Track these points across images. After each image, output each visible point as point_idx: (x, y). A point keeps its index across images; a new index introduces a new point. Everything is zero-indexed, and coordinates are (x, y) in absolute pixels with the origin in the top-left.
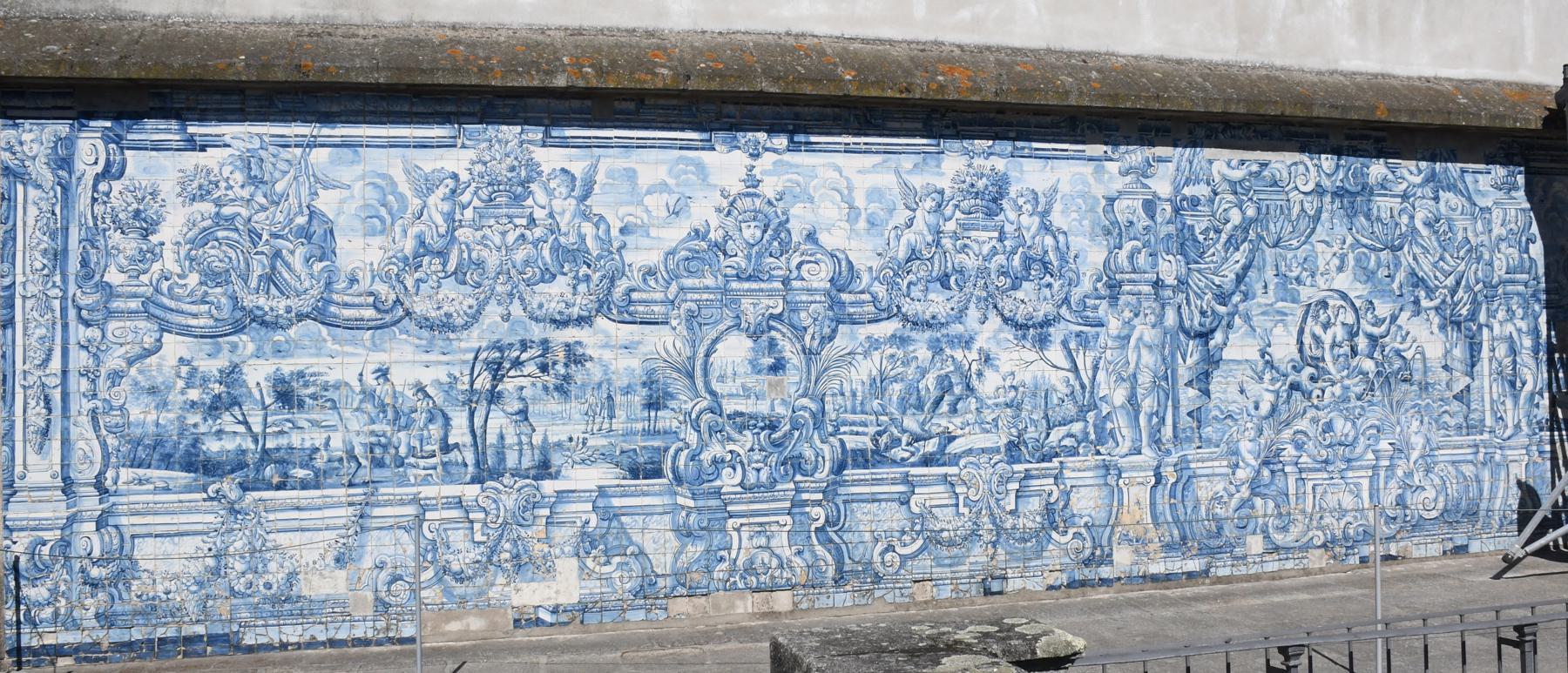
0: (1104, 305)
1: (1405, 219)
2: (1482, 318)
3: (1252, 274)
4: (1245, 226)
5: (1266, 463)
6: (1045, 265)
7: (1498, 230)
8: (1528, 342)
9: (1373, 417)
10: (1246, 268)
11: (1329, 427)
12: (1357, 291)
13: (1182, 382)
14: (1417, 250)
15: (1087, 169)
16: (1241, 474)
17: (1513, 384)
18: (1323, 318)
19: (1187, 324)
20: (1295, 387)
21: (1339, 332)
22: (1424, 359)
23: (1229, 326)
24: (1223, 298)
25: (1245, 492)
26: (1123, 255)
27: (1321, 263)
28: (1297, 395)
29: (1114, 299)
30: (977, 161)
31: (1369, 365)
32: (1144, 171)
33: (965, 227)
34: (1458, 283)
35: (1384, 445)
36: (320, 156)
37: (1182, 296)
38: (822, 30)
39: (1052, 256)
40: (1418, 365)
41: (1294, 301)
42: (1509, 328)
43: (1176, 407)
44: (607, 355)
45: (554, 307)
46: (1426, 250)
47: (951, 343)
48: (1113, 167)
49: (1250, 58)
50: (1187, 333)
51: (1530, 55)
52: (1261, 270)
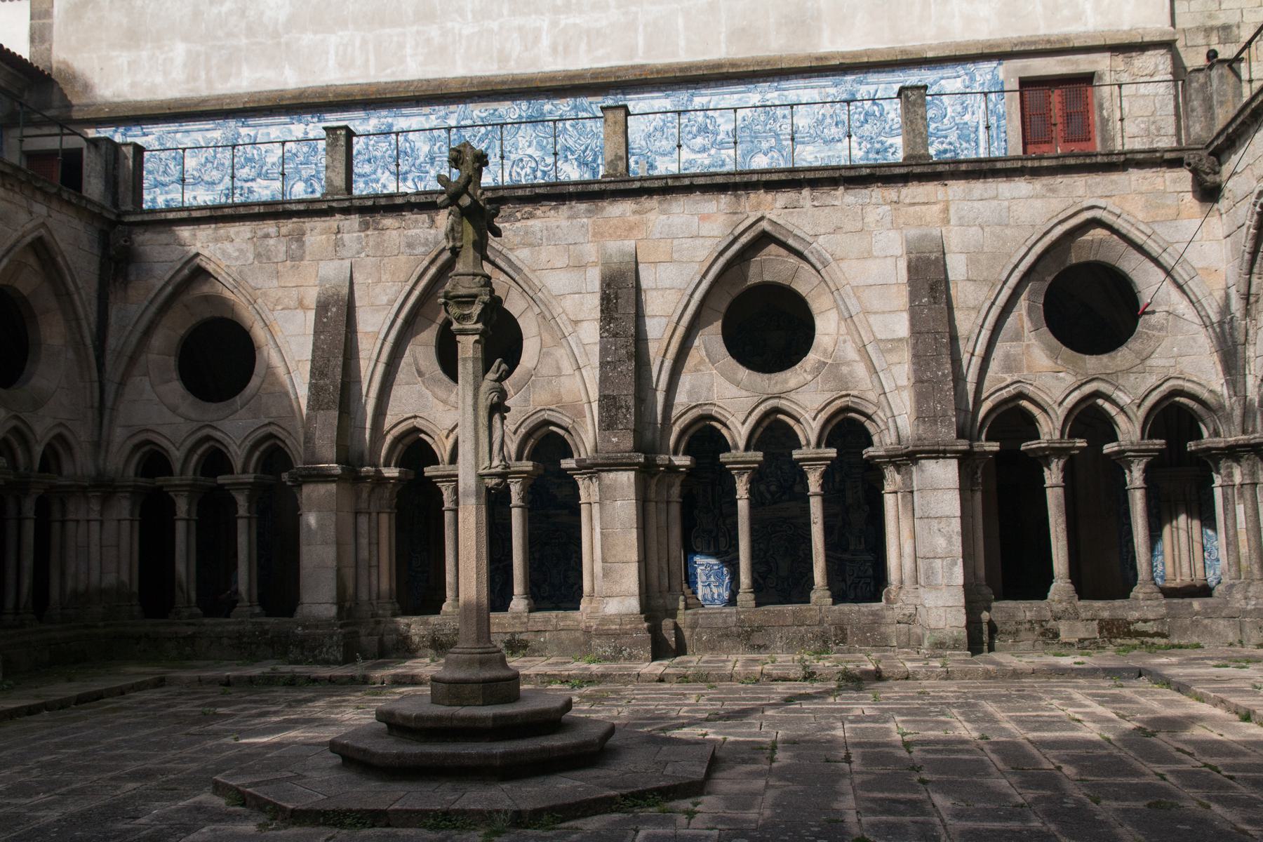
0: (428, 166)
4: (487, 134)
6: (406, 153)
14: (567, 137)
15: (423, 119)
18: (521, 165)
21: (528, 170)
26: (436, 148)
29: (432, 164)
30: (382, 120)
32: (446, 117)
33: (377, 142)
34: (587, 148)
36: (179, 135)
38: (338, 83)
39: (408, 150)
44: (260, 190)
45: (244, 176)
47: (372, 182)
48: (433, 117)
49: (503, 72)
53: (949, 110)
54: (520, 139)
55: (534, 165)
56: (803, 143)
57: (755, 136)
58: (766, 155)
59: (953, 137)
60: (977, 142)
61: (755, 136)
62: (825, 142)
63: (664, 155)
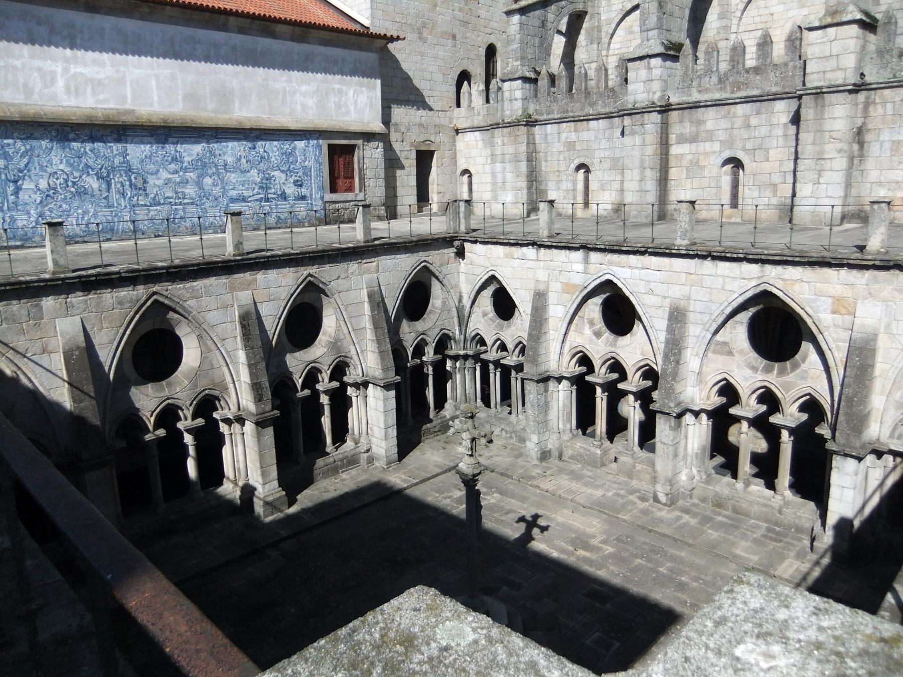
1: (83, 149)
2: (111, 177)
3: (30, 165)
4: (26, 152)
5: (40, 216)
7: (115, 152)
8: (128, 183)
9: (76, 204)
10: (28, 163)
11: (61, 206)
12: (67, 169)
13: (9, 194)
16: (32, 219)
17: (123, 195)
18: (56, 176)
19: (9, 178)
20: (48, 196)
22: (92, 188)
23: (24, 179)
24: (21, 171)
25: (34, 224)
27: (54, 162)
28: (48, 198)
31: (73, 190)
34: (102, 167)
35: (80, 211)
37: (6, 171)
40: (90, 190)
41: (46, 171)
42: (121, 179)
43: (8, 201)
46: (90, 158)
50: (9, 181)
51: (129, 101)
52: (33, 163)
53: (299, 158)
54: (53, 157)
55: (65, 177)
56: (230, 172)
57: (204, 165)
58: (211, 177)
59: (300, 174)
60: (311, 177)
61: (204, 165)
62: (241, 172)
63: (152, 174)
